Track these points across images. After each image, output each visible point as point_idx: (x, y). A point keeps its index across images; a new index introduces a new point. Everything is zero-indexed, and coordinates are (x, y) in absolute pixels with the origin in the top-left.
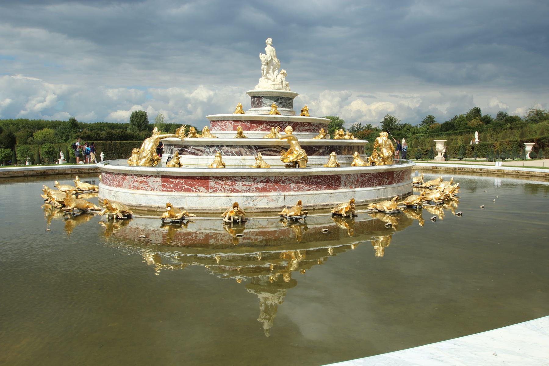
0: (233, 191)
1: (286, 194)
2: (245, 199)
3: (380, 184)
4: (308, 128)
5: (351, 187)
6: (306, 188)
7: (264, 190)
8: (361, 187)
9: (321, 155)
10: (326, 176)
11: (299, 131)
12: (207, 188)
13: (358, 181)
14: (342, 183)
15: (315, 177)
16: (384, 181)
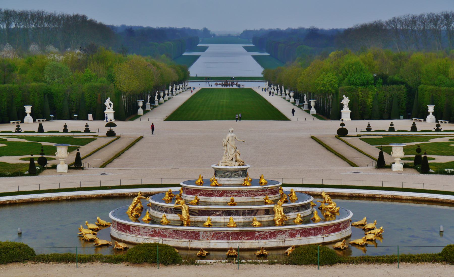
0: (139, 234)
1: (164, 239)
2: (143, 239)
3: (236, 239)
4: (236, 194)
5: (207, 239)
6: (176, 237)
7: (153, 236)
8: (217, 240)
9: (218, 215)
10: (189, 231)
11: (227, 196)
12: (130, 231)
13: (213, 236)
14: (201, 237)
15: (181, 231)
16: (241, 238)
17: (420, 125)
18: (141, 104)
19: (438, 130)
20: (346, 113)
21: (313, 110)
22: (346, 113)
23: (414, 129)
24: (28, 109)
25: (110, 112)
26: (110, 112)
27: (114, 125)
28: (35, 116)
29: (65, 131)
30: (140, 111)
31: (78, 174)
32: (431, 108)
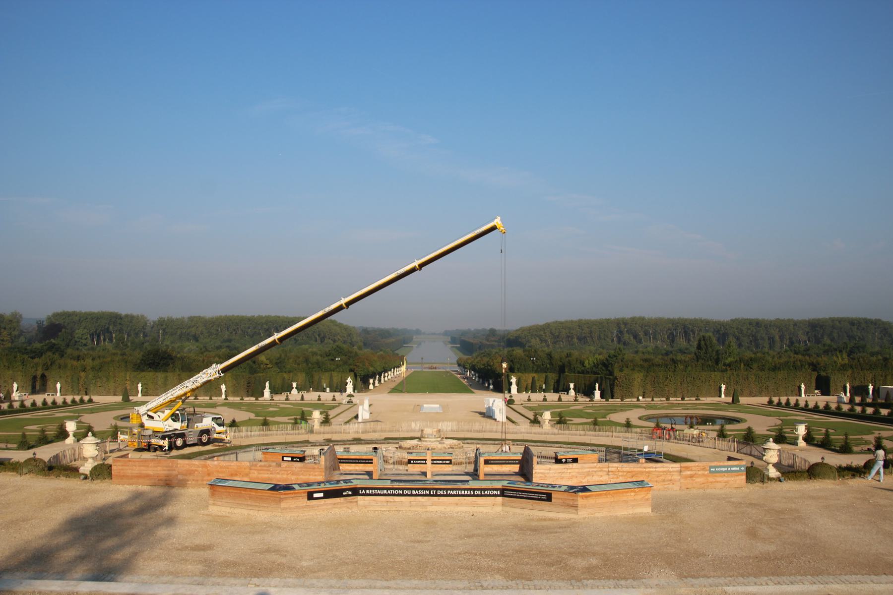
17: (564, 397)
18: (371, 381)
19: (576, 400)
20: (514, 388)
21: (491, 387)
22: (514, 388)
23: (560, 399)
24: (294, 385)
25: (350, 388)
26: (350, 388)
27: (352, 396)
28: (299, 389)
29: (319, 399)
30: (371, 387)
31: (327, 428)
32: (572, 386)
